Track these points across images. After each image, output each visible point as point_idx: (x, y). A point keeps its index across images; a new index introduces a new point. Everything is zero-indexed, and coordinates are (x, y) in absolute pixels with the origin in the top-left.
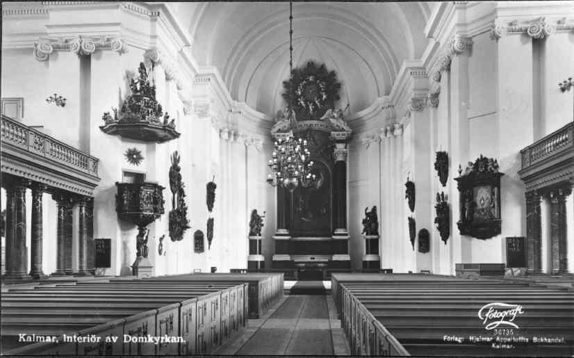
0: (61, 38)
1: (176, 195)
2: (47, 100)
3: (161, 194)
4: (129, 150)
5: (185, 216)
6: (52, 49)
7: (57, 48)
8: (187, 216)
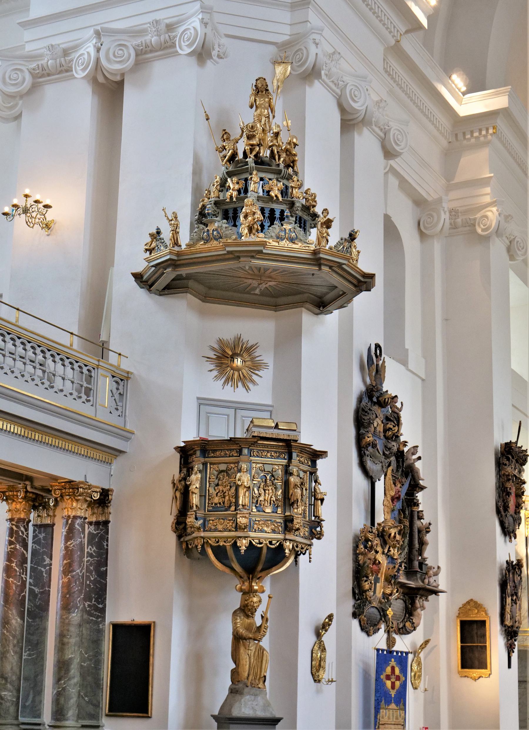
0: (51, 47)
1: (380, 486)
2: (48, 235)
3: (313, 473)
4: (220, 341)
5: (420, 552)
6: (28, 78)
7: (43, 76)
8: (426, 554)
